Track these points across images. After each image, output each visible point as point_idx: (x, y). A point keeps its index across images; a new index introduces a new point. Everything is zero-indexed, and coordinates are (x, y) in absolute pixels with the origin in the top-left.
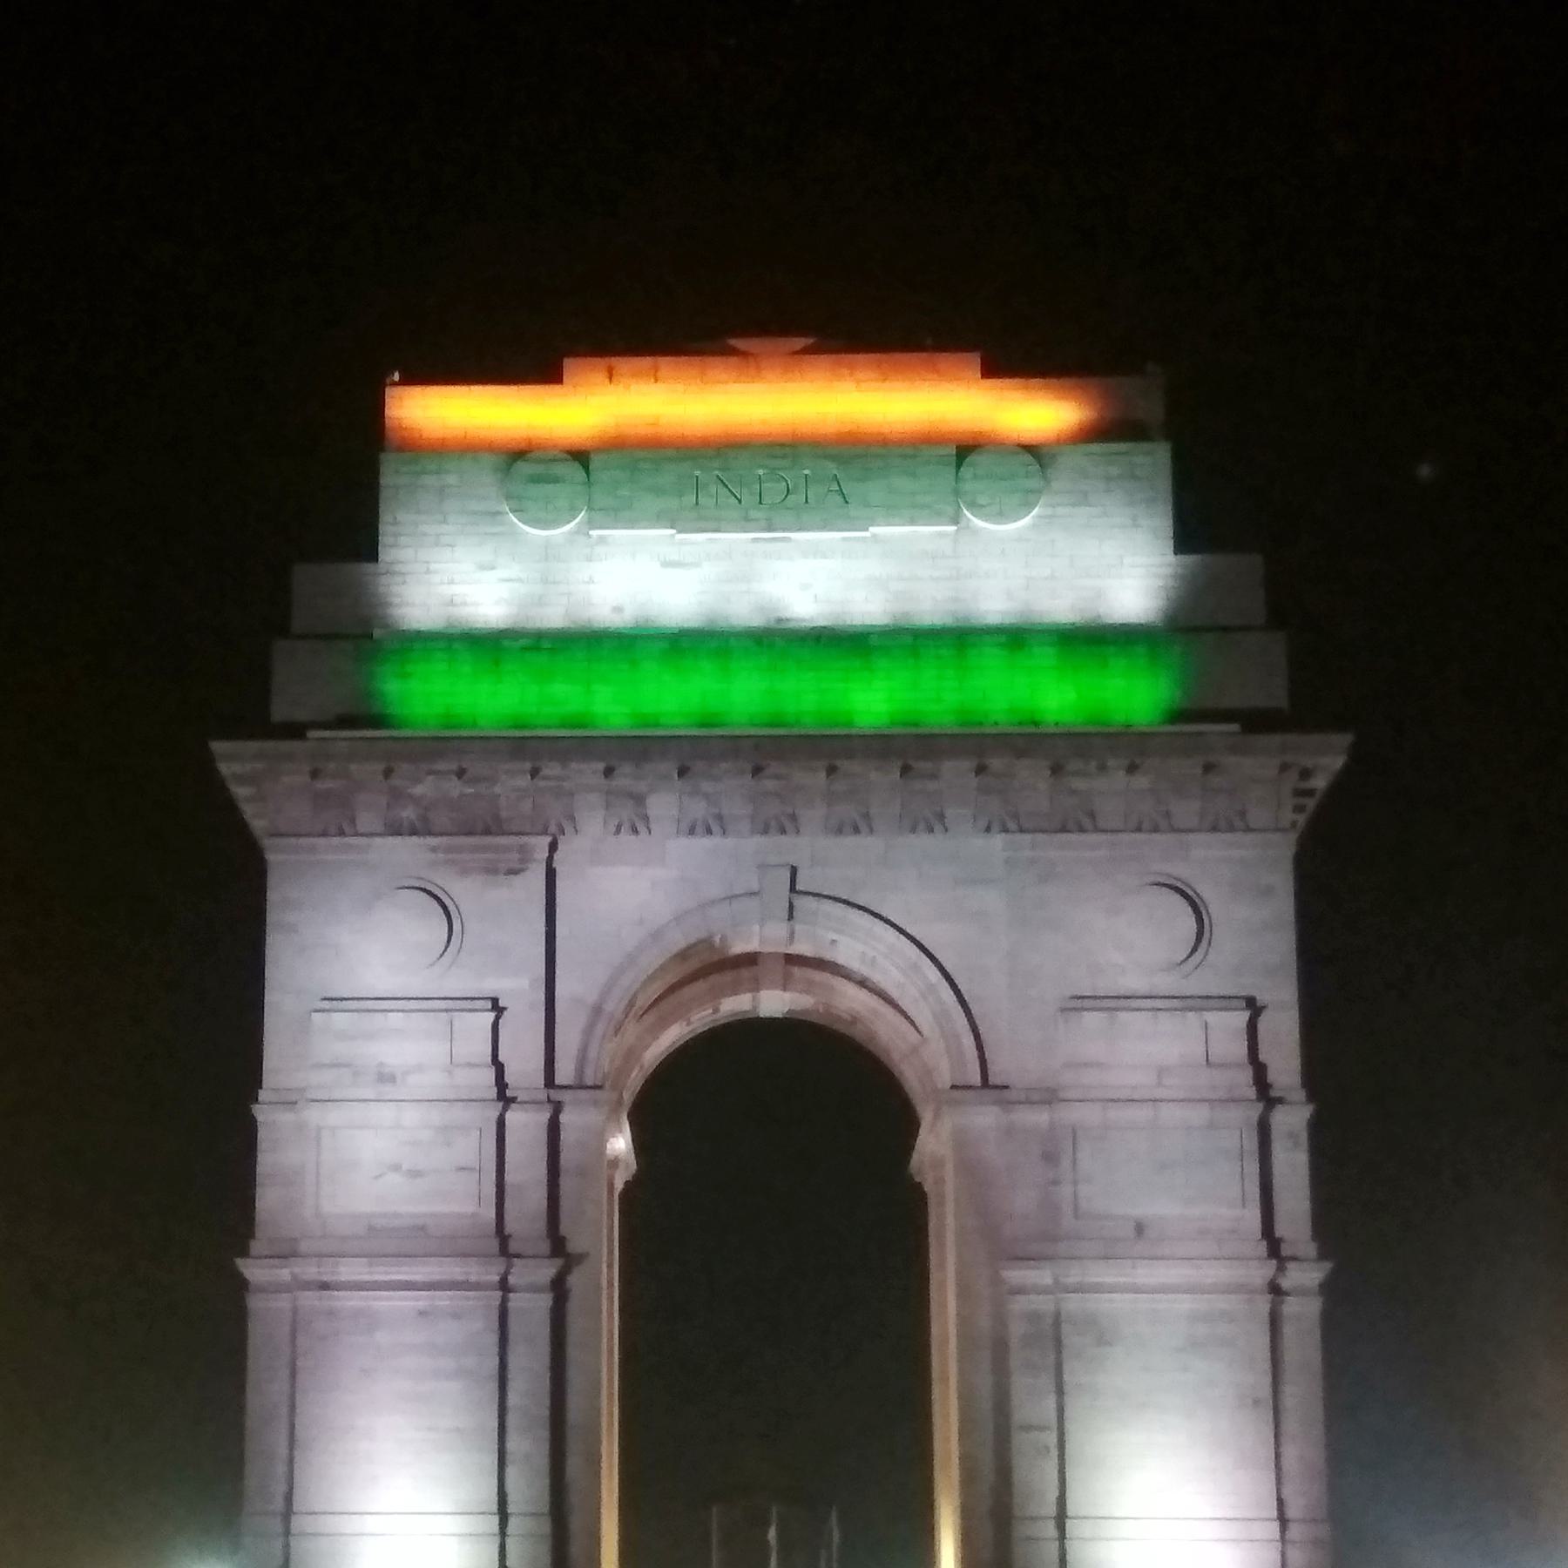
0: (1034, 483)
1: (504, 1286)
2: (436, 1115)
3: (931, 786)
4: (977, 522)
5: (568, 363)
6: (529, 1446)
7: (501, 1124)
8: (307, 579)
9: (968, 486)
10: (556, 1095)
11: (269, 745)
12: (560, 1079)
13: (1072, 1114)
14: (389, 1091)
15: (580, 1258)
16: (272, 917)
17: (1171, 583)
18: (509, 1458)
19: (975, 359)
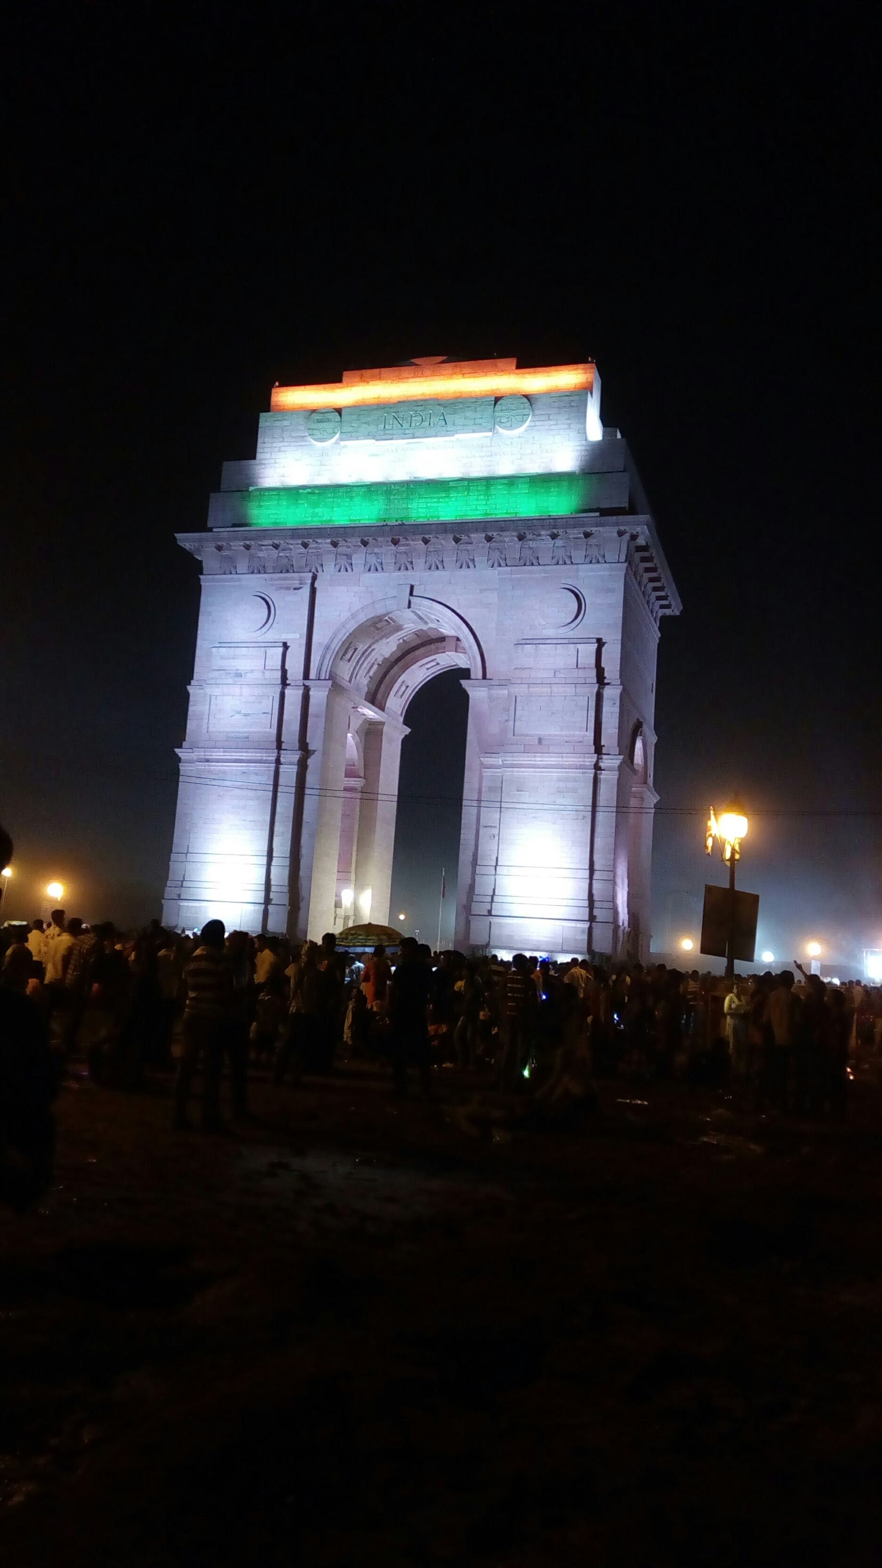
0: (526, 412)
1: (278, 762)
2: (257, 691)
3: (469, 547)
4: (501, 430)
6: (283, 830)
8: (229, 467)
9: (497, 414)
10: (307, 683)
11: (196, 535)
12: (311, 677)
13: (519, 690)
14: (239, 679)
16: (202, 609)
17: (586, 453)
18: (275, 834)
19: (514, 361)
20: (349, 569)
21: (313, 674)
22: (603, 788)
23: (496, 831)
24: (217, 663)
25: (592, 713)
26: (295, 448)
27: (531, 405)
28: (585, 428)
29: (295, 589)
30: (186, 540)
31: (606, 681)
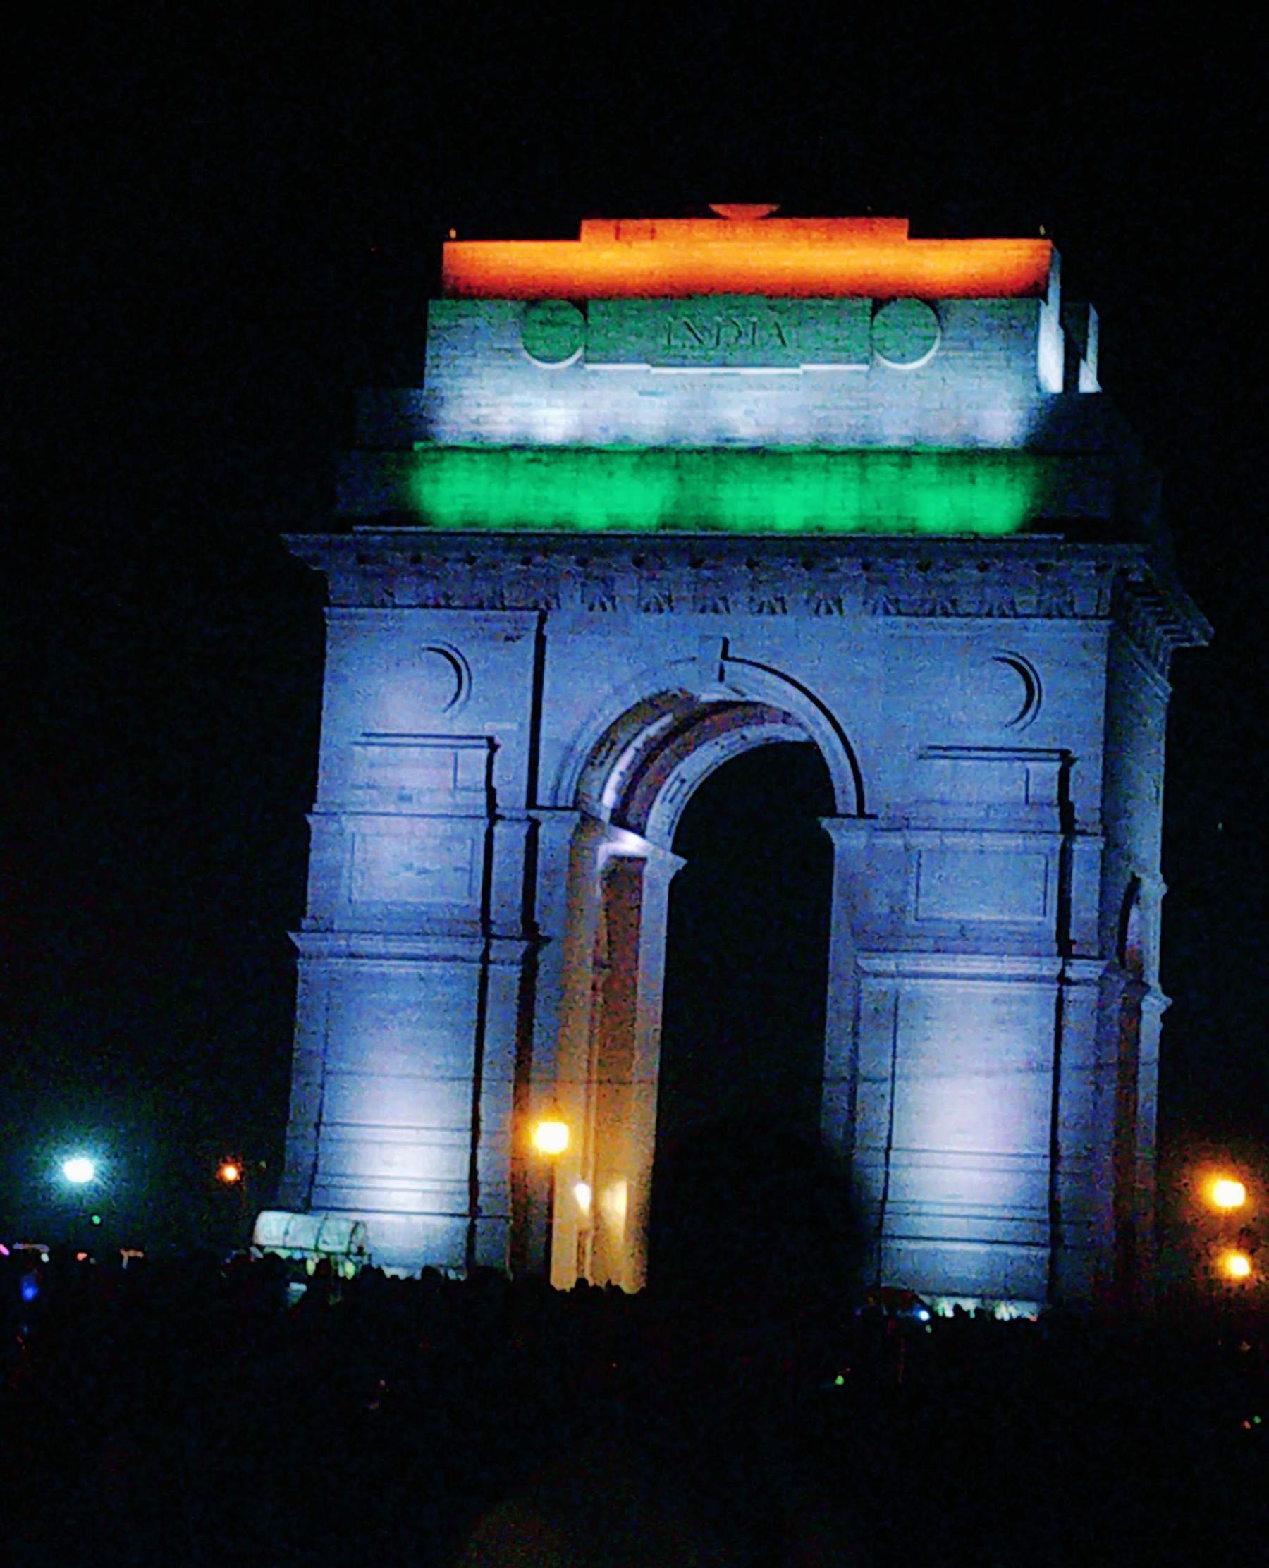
1: (485, 960)
2: (441, 827)
5: (585, 225)
7: (489, 836)
12: (540, 801)
14: (406, 808)
15: (548, 940)
20: (608, 605)
21: (543, 798)
22: (1071, 1017)
23: (886, 1087)
24: (361, 774)
25: (1054, 887)
26: (497, 371)
27: (939, 317)
28: (1035, 368)
29: (508, 639)
30: (302, 544)
31: (1077, 827)
